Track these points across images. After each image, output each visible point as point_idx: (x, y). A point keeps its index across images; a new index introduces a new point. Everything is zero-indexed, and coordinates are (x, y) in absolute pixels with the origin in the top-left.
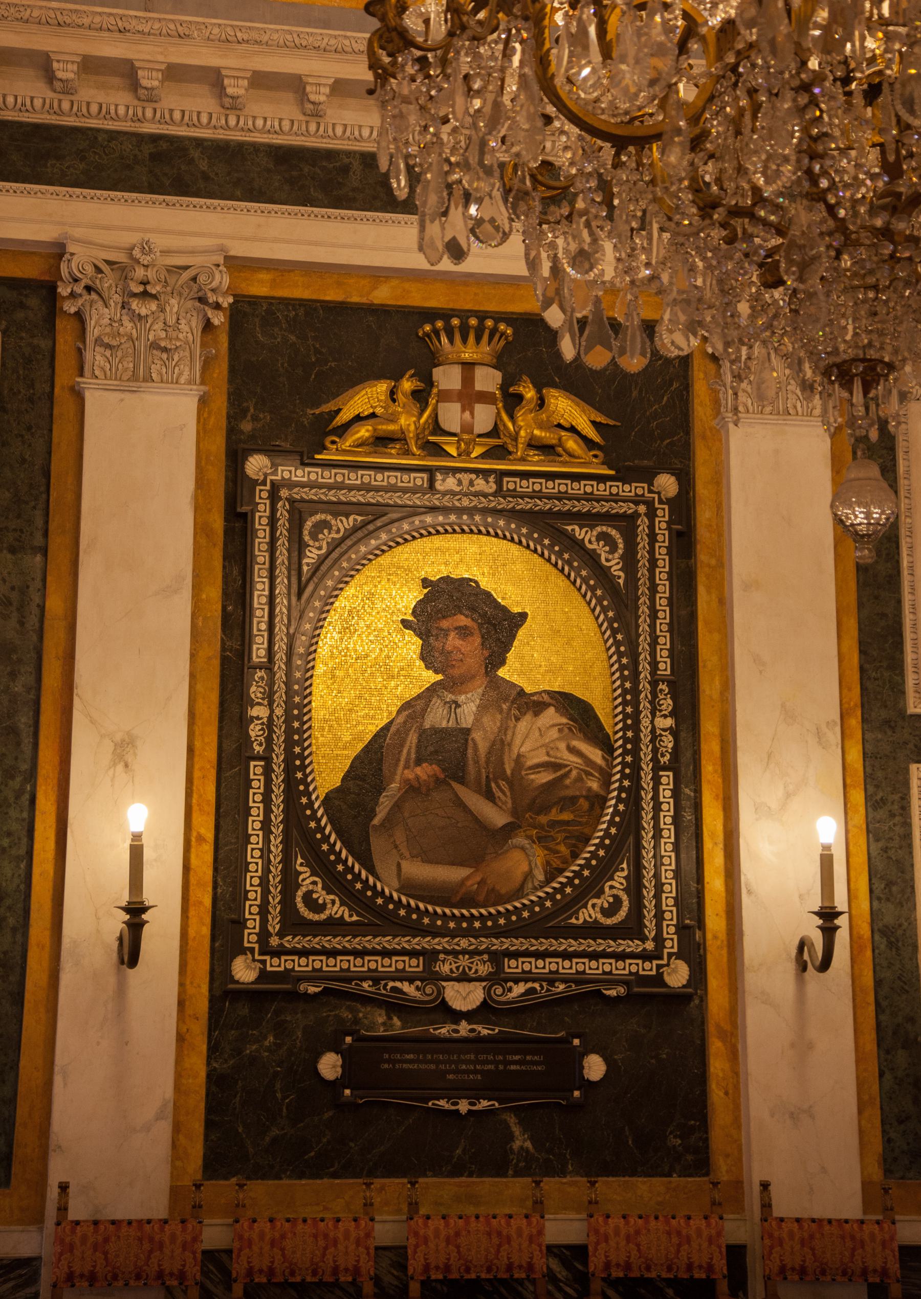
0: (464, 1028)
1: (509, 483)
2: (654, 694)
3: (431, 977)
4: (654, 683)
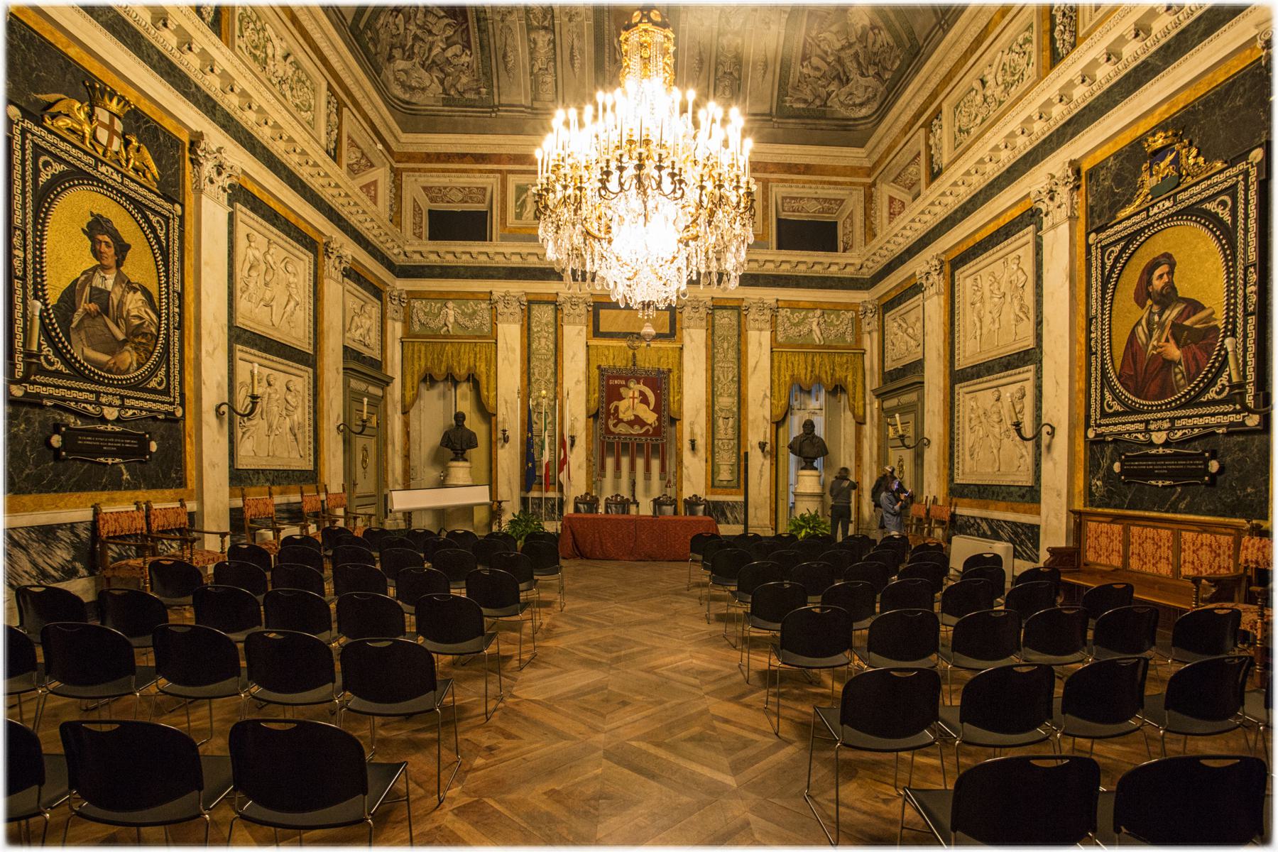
0: (1161, 450)
1: (1180, 197)
2: (1245, 275)
3: (1147, 431)
4: (1246, 269)
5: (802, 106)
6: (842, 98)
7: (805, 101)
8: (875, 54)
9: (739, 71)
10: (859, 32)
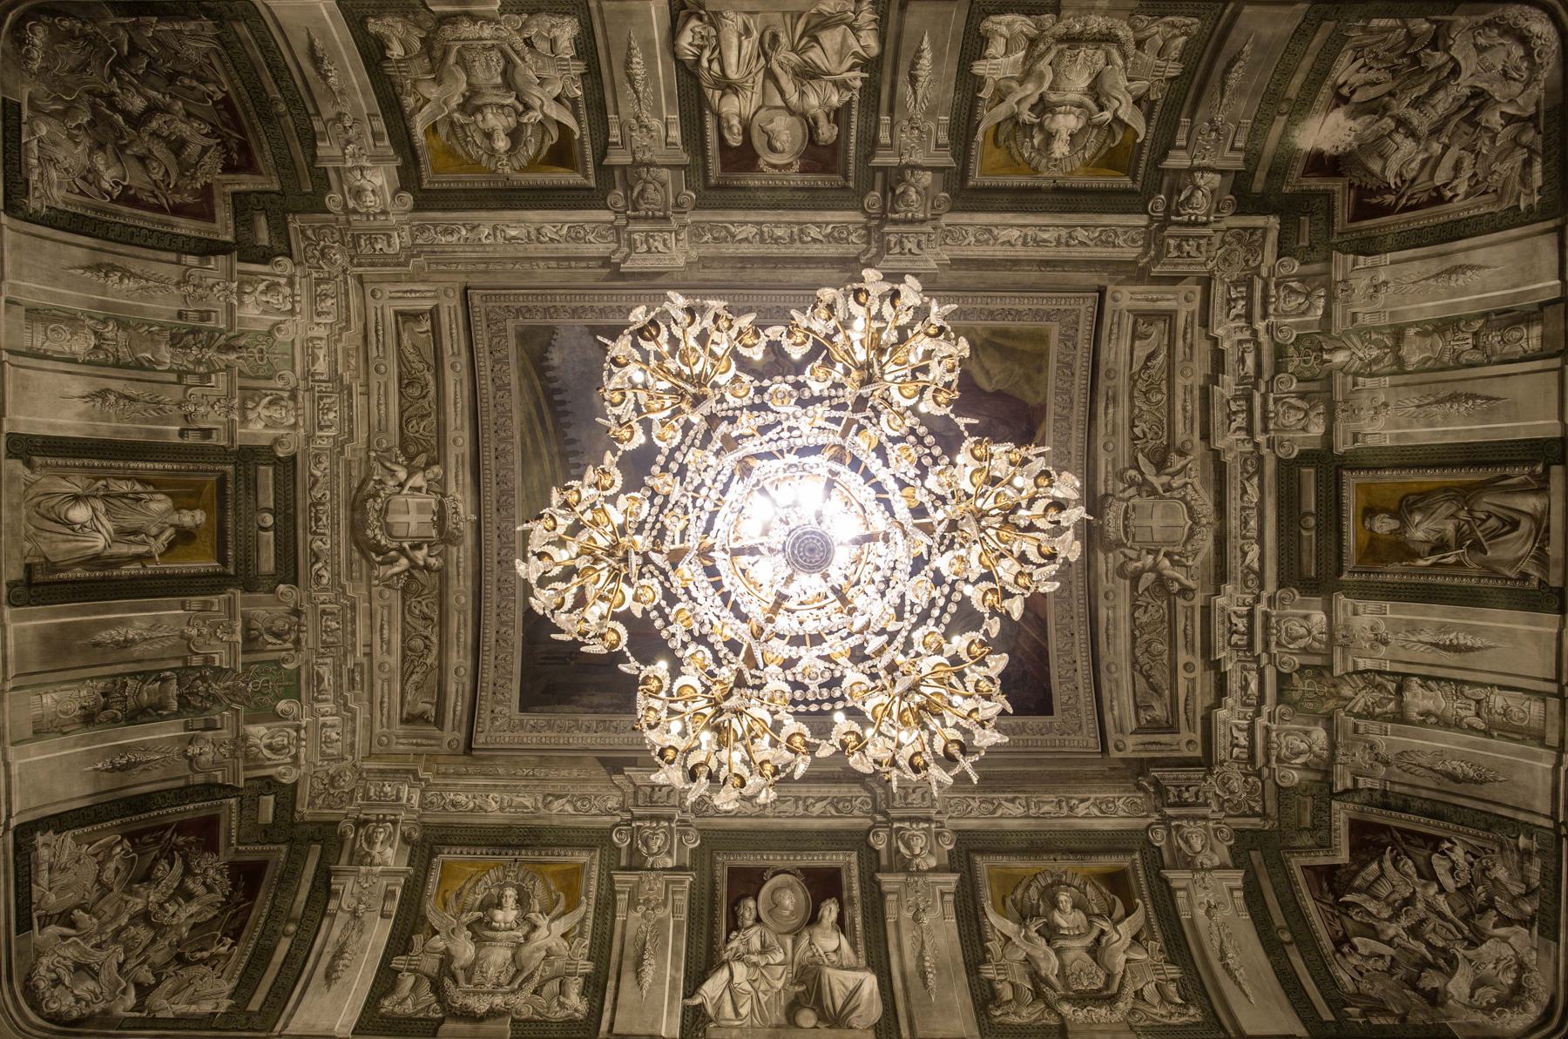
5: (1537, 167)
6: (1516, 88)
7: (1527, 164)
8: (1394, 71)
9: (1469, 319)
10: (1368, 118)
